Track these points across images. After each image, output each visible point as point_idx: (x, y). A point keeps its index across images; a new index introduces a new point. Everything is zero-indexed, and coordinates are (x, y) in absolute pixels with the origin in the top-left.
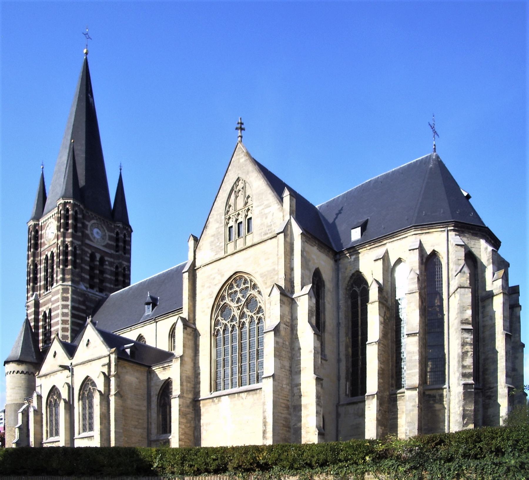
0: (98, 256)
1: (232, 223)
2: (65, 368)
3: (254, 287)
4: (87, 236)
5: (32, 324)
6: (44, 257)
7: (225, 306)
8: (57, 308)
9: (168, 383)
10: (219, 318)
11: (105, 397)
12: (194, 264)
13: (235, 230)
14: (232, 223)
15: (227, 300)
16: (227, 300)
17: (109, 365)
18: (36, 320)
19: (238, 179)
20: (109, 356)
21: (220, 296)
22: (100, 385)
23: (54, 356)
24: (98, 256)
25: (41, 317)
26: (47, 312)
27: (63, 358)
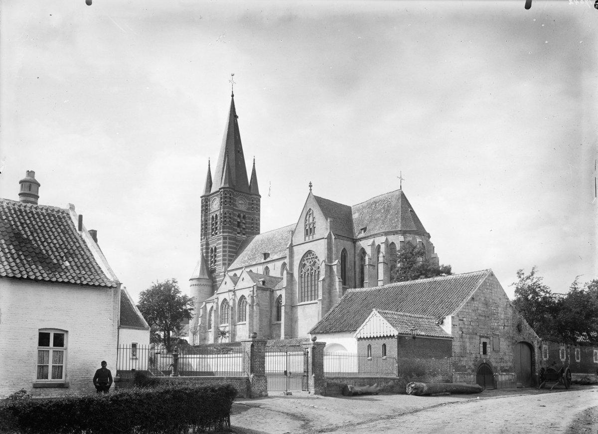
0: (242, 215)
1: (307, 228)
2: (230, 291)
3: (317, 257)
4: (235, 205)
5: (204, 255)
6: (211, 217)
7: (305, 264)
8: (220, 248)
9: (281, 295)
10: (302, 269)
11: (252, 306)
12: (292, 244)
13: (309, 231)
14: (307, 228)
15: (305, 262)
16: (305, 262)
17: (253, 291)
18: (207, 253)
19: (310, 209)
20: (253, 287)
21: (302, 260)
22: (249, 300)
23: (225, 284)
24: (242, 215)
25: (210, 250)
26: (213, 248)
27: (230, 285)
